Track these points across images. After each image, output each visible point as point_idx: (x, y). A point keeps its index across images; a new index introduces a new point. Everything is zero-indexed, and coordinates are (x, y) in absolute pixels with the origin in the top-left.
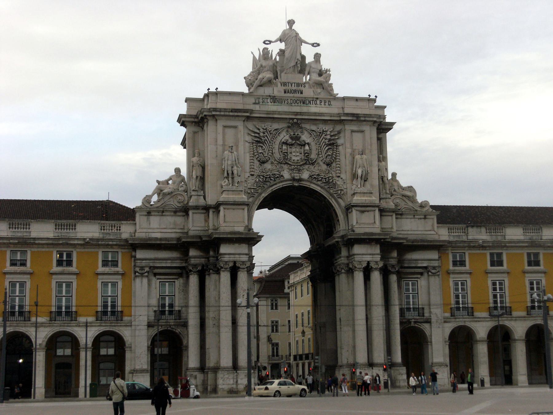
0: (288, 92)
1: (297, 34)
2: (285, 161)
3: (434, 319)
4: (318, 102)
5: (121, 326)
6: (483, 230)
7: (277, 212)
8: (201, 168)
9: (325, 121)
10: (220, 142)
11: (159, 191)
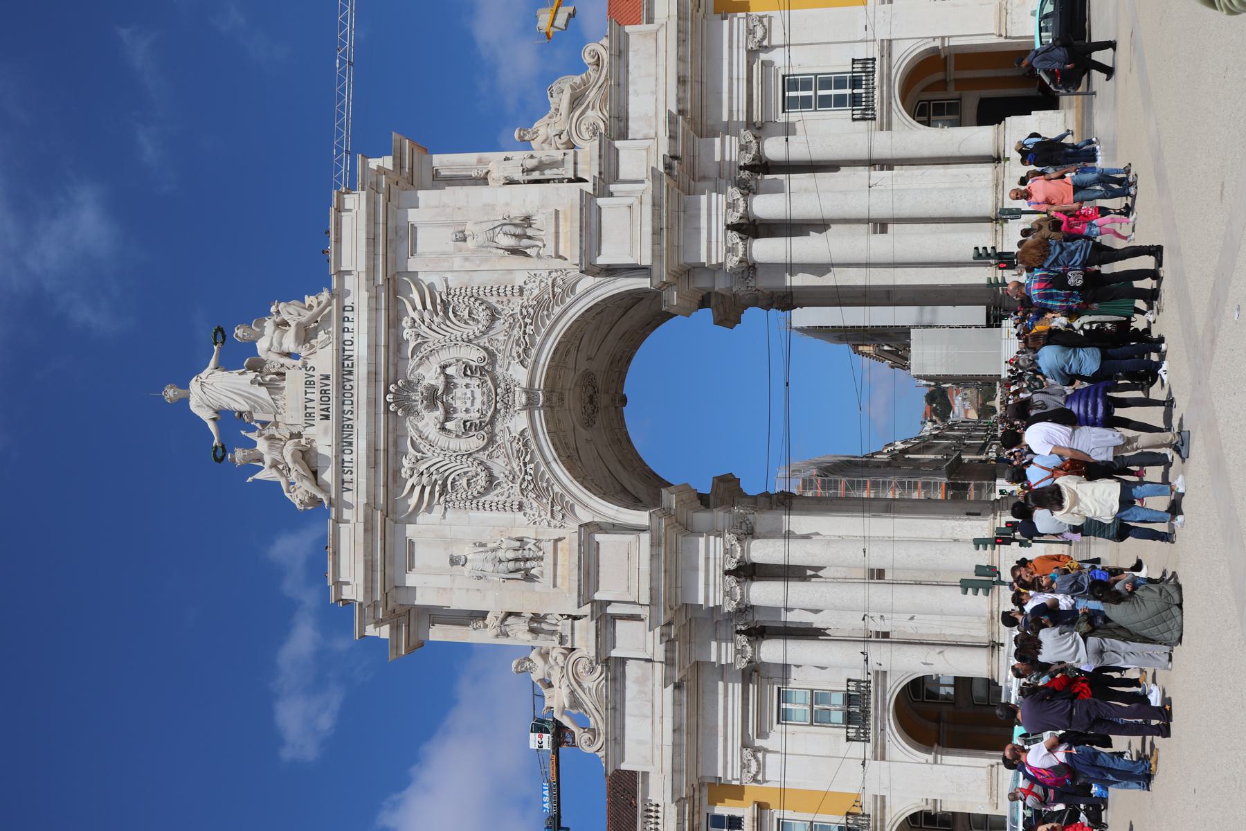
0: (327, 410)
3: (883, 34)
4: (347, 336)
5: (883, 820)
8: (510, 620)
10: (445, 581)
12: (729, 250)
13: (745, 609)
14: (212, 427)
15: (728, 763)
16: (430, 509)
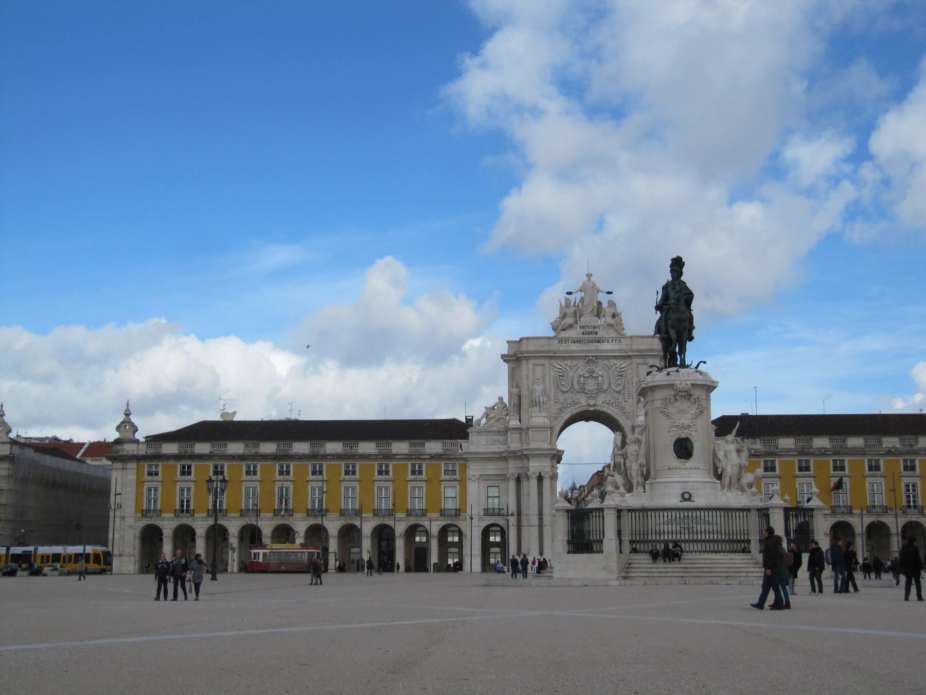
1: (594, 285)
6: (758, 441)
7: (592, 424)
9: (615, 357)
11: (487, 415)
13: (528, 478)
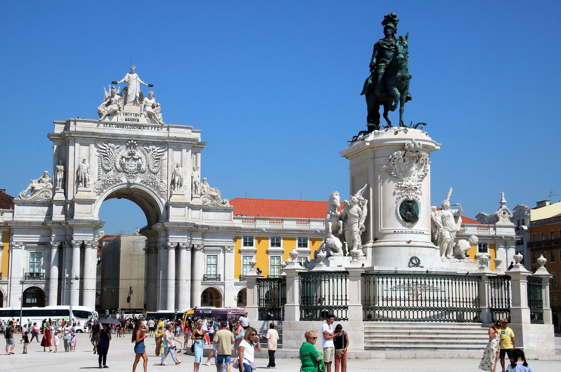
2: (123, 169)
4: (150, 128)
12: (172, 243)
13: (71, 246)
14: (123, 80)
15: (17, 238)
16: (98, 151)
